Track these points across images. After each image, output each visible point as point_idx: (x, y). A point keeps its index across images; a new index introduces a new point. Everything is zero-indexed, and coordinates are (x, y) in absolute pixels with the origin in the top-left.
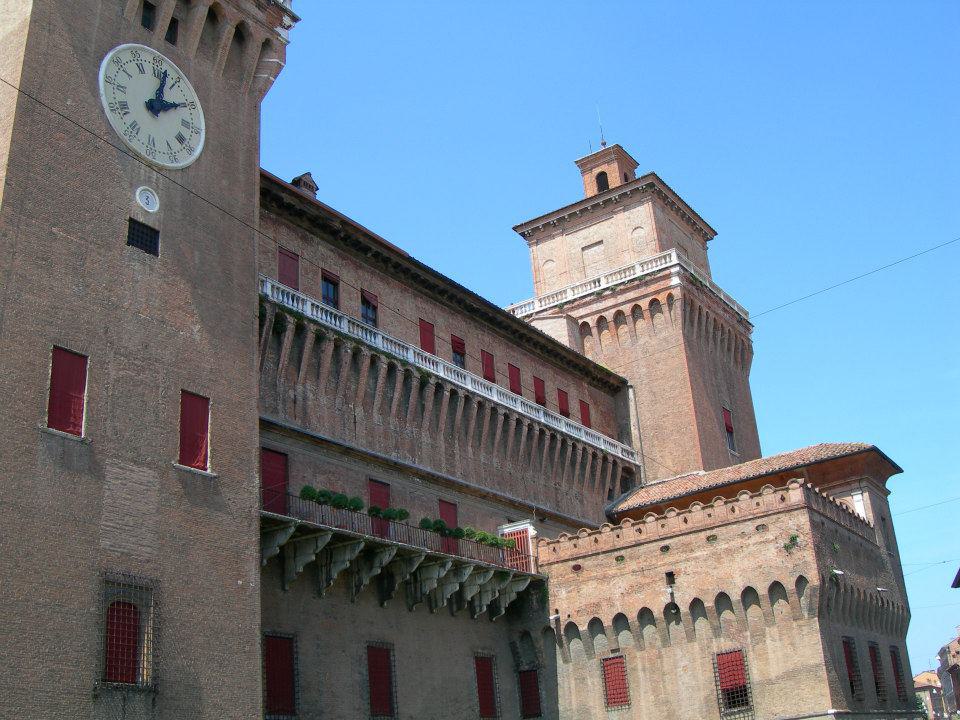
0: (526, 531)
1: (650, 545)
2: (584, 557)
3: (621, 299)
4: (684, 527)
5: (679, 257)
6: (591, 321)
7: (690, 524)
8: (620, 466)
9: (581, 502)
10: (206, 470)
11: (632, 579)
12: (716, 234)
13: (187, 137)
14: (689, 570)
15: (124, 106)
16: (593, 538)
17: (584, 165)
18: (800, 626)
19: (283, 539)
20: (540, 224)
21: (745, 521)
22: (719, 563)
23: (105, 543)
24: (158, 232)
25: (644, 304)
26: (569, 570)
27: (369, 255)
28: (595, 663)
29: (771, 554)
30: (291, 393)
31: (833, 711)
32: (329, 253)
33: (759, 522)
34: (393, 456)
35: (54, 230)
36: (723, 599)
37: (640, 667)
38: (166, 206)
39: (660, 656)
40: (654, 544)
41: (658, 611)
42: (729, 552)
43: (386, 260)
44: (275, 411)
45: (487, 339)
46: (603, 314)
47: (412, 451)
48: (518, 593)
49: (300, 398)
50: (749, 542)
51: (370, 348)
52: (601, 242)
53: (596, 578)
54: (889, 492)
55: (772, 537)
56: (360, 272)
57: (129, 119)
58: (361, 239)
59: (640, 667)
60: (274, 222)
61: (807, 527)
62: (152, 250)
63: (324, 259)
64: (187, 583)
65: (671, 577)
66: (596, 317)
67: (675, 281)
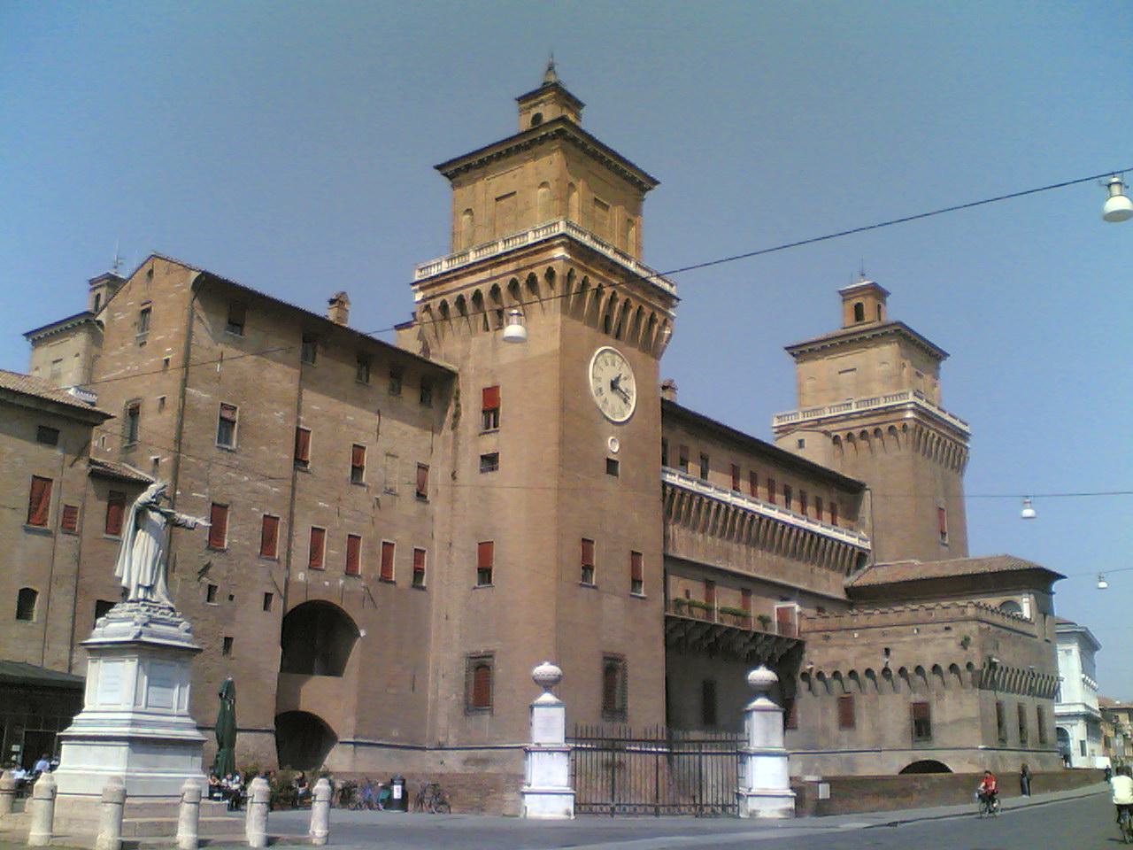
0: (793, 608)
3: (866, 421)
4: (900, 620)
5: (915, 394)
6: (842, 435)
8: (857, 551)
11: (863, 649)
15: (600, 389)
17: (846, 295)
19: (671, 626)
20: (806, 349)
25: (884, 428)
29: (952, 646)
39: (877, 699)
41: (877, 672)
42: (926, 641)
46: (852, 431)
47: (728, 560)
51: (708, 497)
52: (854, 370)
54: (1052, 593)
55: (953, 636)
57: (603, 397)
59: (864, 704)
61: (976, 633)
65: (887, 651)
66: (846, 432)
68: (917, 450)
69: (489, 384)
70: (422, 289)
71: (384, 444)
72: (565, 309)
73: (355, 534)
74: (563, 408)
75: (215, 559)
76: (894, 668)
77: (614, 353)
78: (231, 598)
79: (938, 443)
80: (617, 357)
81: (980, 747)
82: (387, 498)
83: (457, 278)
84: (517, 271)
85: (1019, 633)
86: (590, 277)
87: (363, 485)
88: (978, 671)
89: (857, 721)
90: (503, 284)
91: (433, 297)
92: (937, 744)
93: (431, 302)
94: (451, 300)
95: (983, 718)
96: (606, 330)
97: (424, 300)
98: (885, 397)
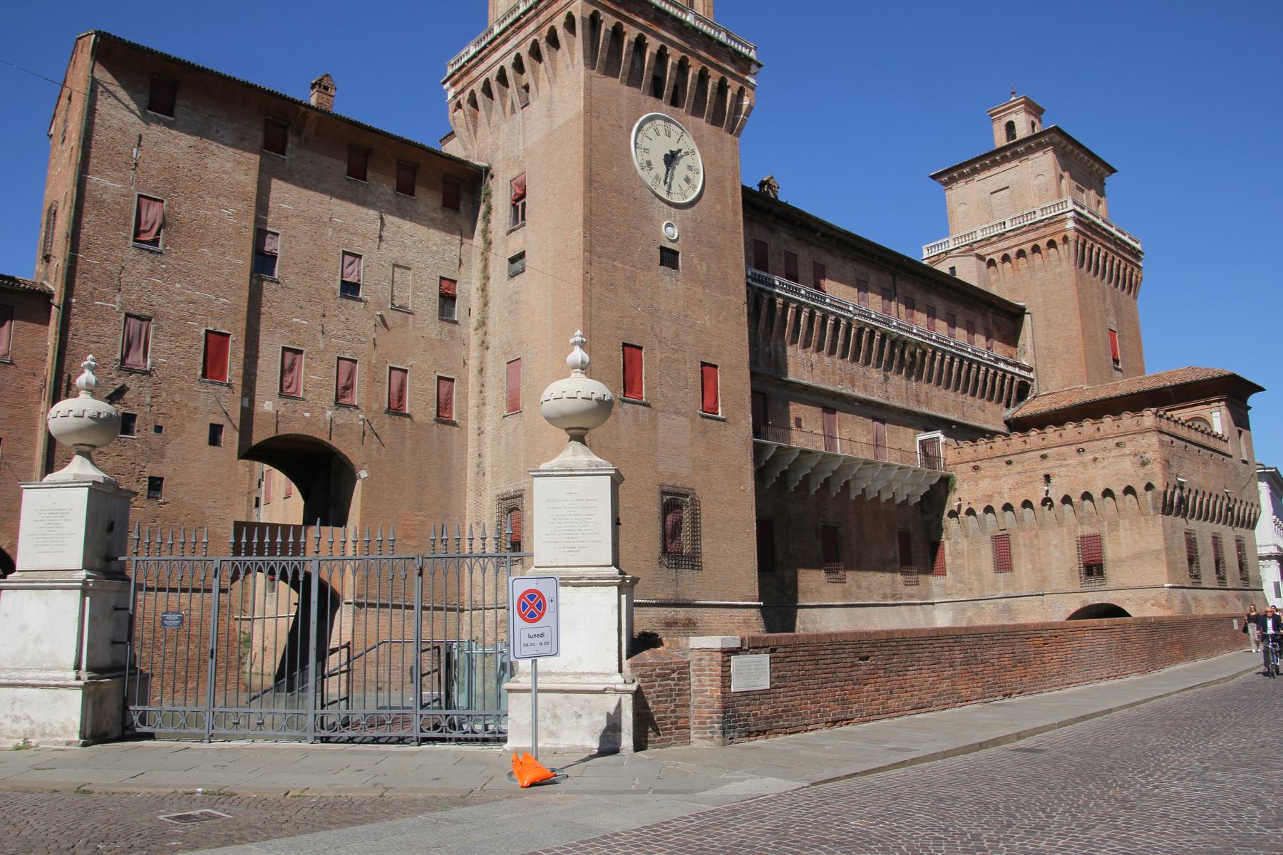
1: (1032, 453)
2: (981, 460)
3: (1023, 239)
4: (1059, 441)
7: (1064, 440)
8: (1017, 379)
9: (983, 411)
10: (717, 414)
12: (1113, 171)
13: (691, 177)
14: (1061, 474)
15: (649, 163)
16: (989, 445)
18: (1146, 520)
21: (1107, 438)
22: (1086, 470)
23: (661, 468)
25: (1042, 244)
26: (970, 469)
27: (818, 235)
28: (988, 538)
30: (767, 349)
31: (1169, 585)
32: (789, 237)
33: (1118, 440)
36: (1087, 496)
37: (1021, 543)
38: (683, 232)
39: (1037, 536)
40: (1036, 453)
43: (831, 237)
45: (909, 287)
46: (1007, 252)
48: (931, 486)
49: (773, 352)
50: (1112, 454)
52: (1008, 187)
53: (990, 476)
55: (1128, 453)
56: (812, 248)
57: (653, 173)
58: (813, 224)
61: (1156, 446)
62: (674, 265)
64: (709, 489)
65: (1047, 478)
66: (1001, 254)
67: (1070, 224)
68: (1082, 266)
69: (516, 173)
70: (453, 85)
71: (391, 252)
72: (591, 59)
73: (347, 356)
74: (590, 181)
75: (132, 382)
76: (1056, 497)
77: (667, 120)
78: (158, 429)
79: (1105, 258)
80: (673, 126)
81: (1166, 585)
82: (394, 318)
83: (482, 60)
84: (538, 28)
85: (1210, 448)
86: (624, 24)
87: (360, 300)
88: (1159, 493)
89: (1014, 562)
90: (524, 51)
91: (463, 90)
92: (1111, 583)
93: (460, 96)
94: (478, 87)
95: (1169, 549)
96: (657, 91)
97: (455, 97)
98: (1042, 210)
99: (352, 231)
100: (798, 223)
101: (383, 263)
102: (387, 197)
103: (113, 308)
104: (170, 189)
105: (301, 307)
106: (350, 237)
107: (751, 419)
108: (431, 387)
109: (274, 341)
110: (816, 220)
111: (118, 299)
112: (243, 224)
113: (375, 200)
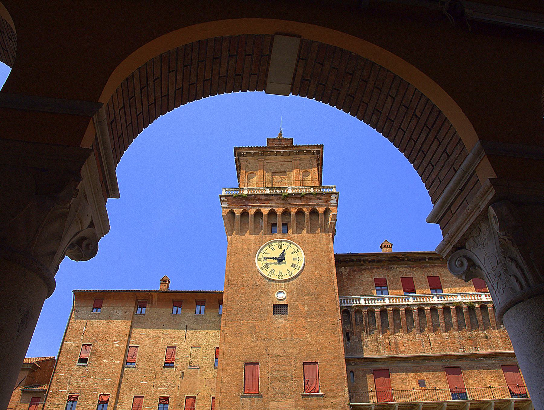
24: (287, 305)
27: (427, 260)
34: (460, 352)
35: (242, 322)
38: (290, 293)
44: (379, 351)
49: (392, 341)
56: (426, 269)
58: (418, 256)
60: (370, 269)
63: (401, 273)
77: (278, 241)
99: (172, 337)
100: (406, 259)
101: (186, 348)
102: (190, 318)
103: (65, 392)
104: (95, 339)
105: (145, 376)
106: (171, 340)
107: (347, 391)
108: (208, 403)
109: (131, 394)
110: (418, 253)
111: (67, 388)
112: (122, 346)
113: (184, 321)
